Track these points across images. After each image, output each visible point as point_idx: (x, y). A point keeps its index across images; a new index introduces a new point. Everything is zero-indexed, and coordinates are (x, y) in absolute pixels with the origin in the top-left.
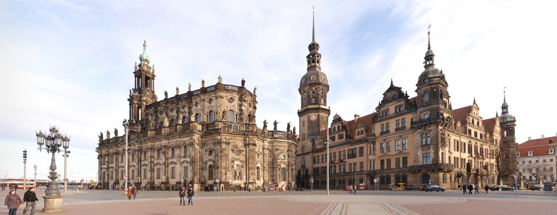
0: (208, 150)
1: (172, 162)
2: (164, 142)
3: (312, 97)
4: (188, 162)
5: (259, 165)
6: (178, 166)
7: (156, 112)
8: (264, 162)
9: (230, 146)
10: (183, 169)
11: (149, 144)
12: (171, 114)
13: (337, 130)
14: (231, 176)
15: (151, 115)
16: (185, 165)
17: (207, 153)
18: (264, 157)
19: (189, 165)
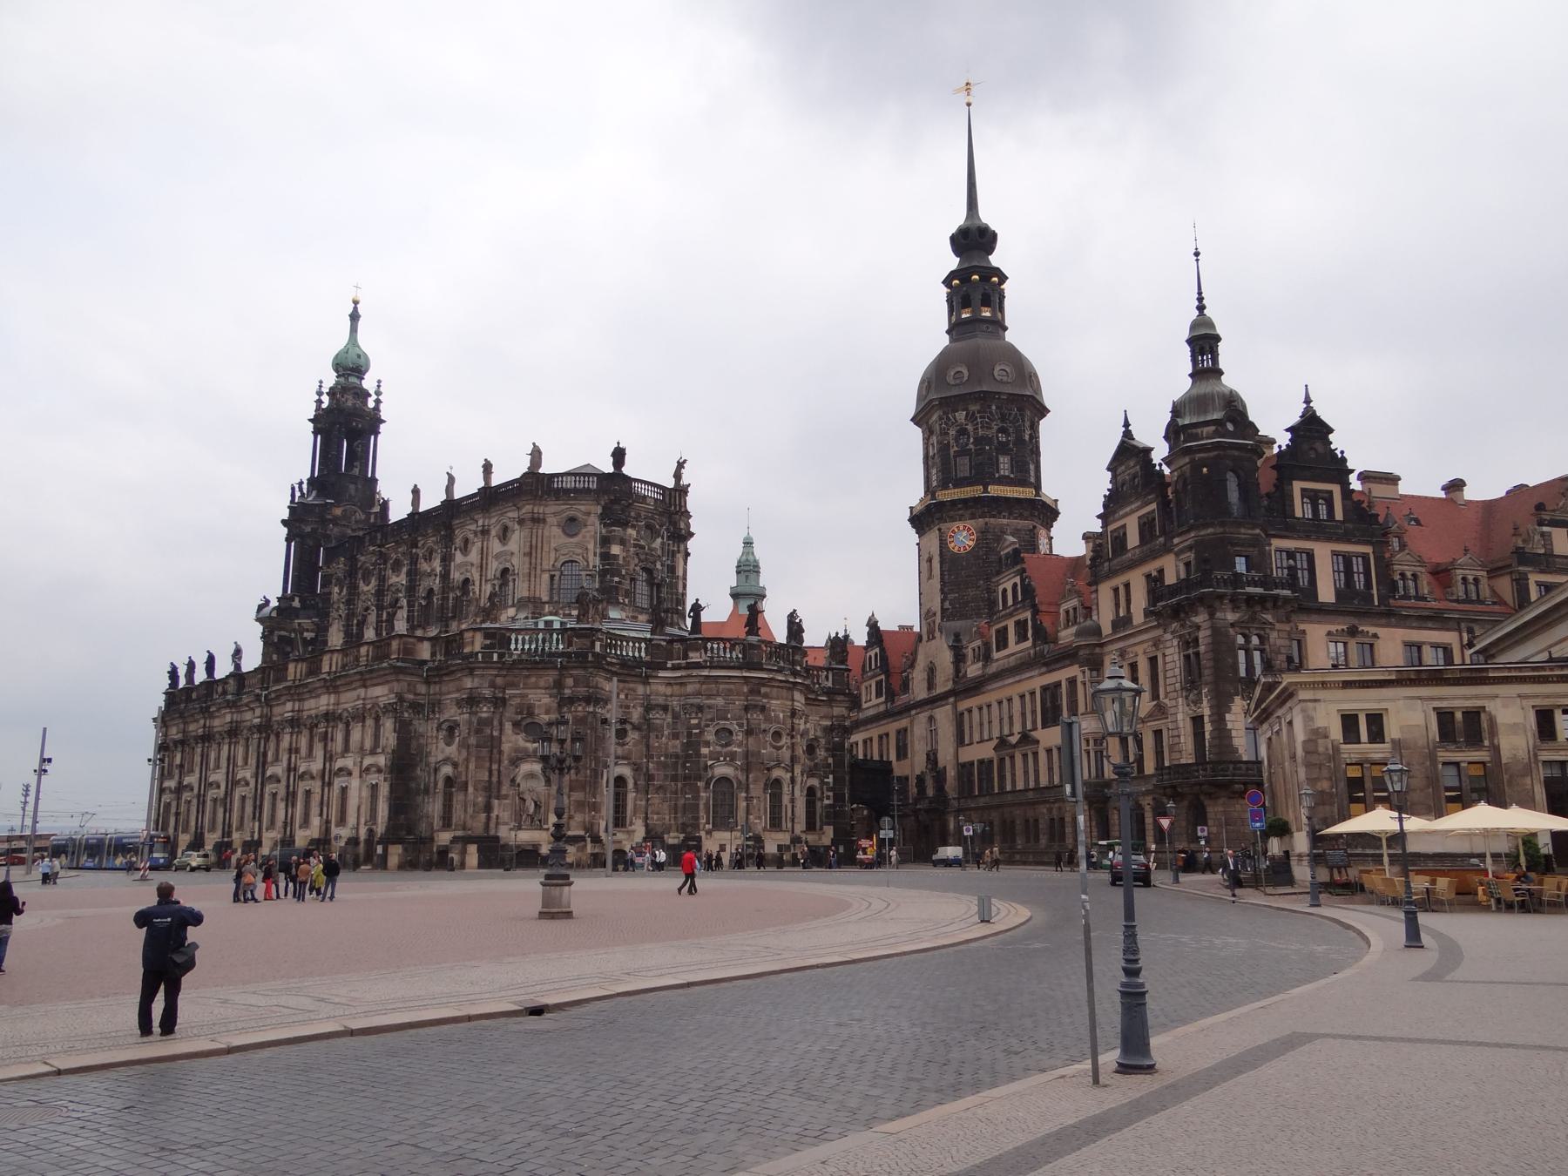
0: (445, 726)
1: (341, 769)
2: (324, 702)
3: (957, 454)
4: (379, 771)
5: (626, 771)
6: (354, 783)
7: (352, 573)
8: (649, 757)
9: (510, 713)
10: (366, 793)
11: (289, 706)
12: (394, 579)
13: (1010, 602)
14: (505, 815)
15: (340, 583)
16: (373, 778)
17: (442, 734)
18: (647, 737)
19: (382, 777)
